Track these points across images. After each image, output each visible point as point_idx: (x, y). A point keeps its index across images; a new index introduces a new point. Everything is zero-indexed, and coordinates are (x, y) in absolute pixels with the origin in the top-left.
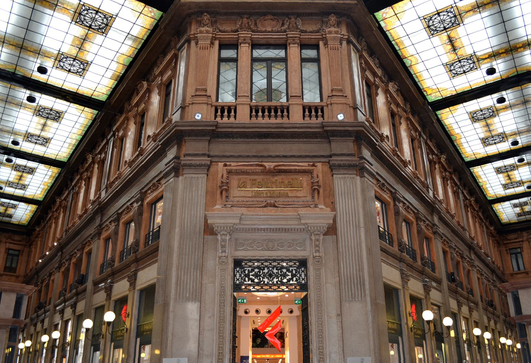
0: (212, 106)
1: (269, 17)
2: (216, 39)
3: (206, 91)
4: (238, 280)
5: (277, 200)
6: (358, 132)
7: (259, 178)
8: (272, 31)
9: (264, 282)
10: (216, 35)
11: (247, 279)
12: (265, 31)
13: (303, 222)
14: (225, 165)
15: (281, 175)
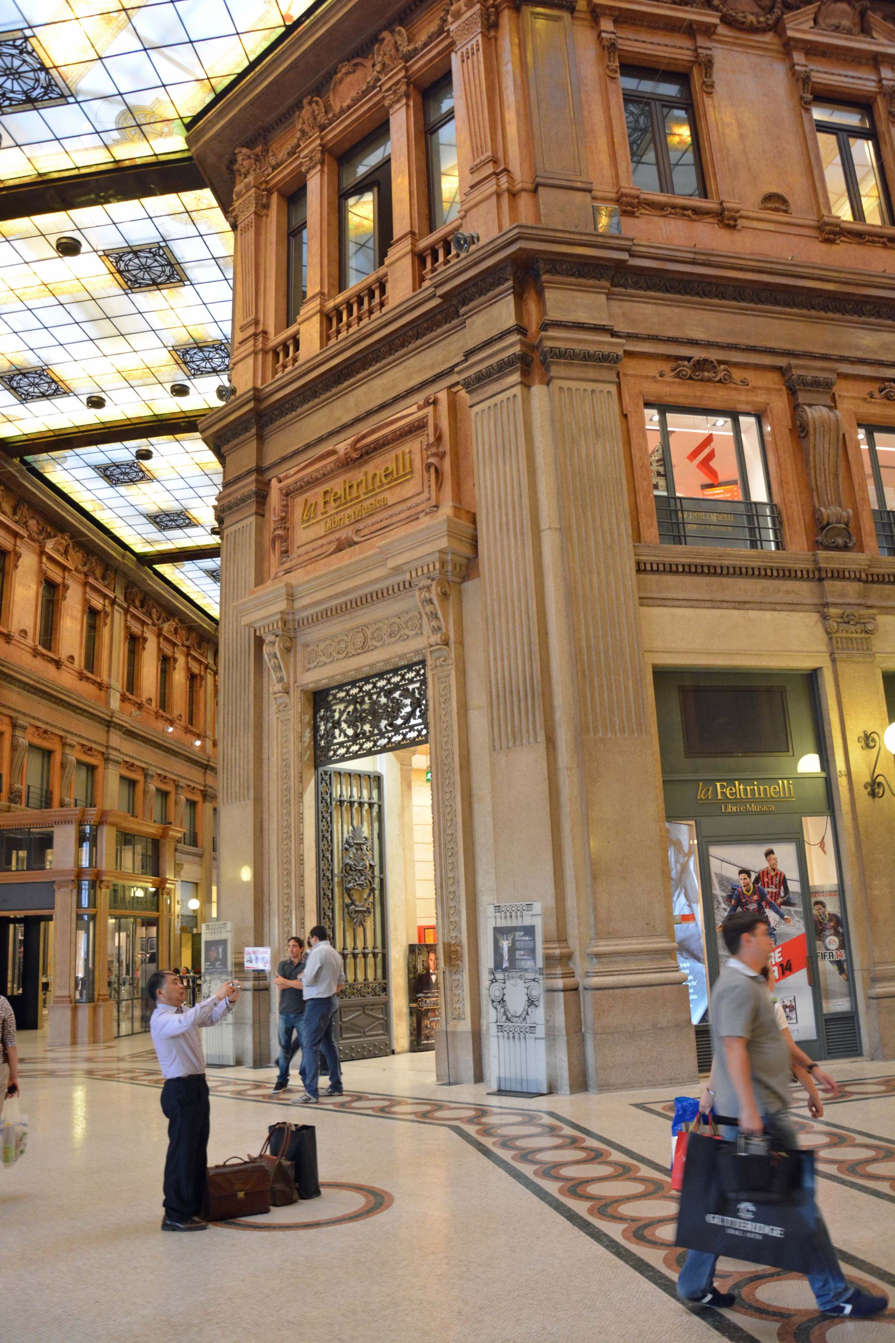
0: (265, 352)
1: (344, 70)
2: (270, 192)
3: (256, 322)
4: (322, 737)
5: (360, 525)
6: (514, 259)
7: (337, 485)
8: (355, 101)
9: (364, 733)
10: (267, 182)
11: (337, 732)
12: (343, 111)
13: (391, 564)
14: (280, 481)
15: (373, 458)
